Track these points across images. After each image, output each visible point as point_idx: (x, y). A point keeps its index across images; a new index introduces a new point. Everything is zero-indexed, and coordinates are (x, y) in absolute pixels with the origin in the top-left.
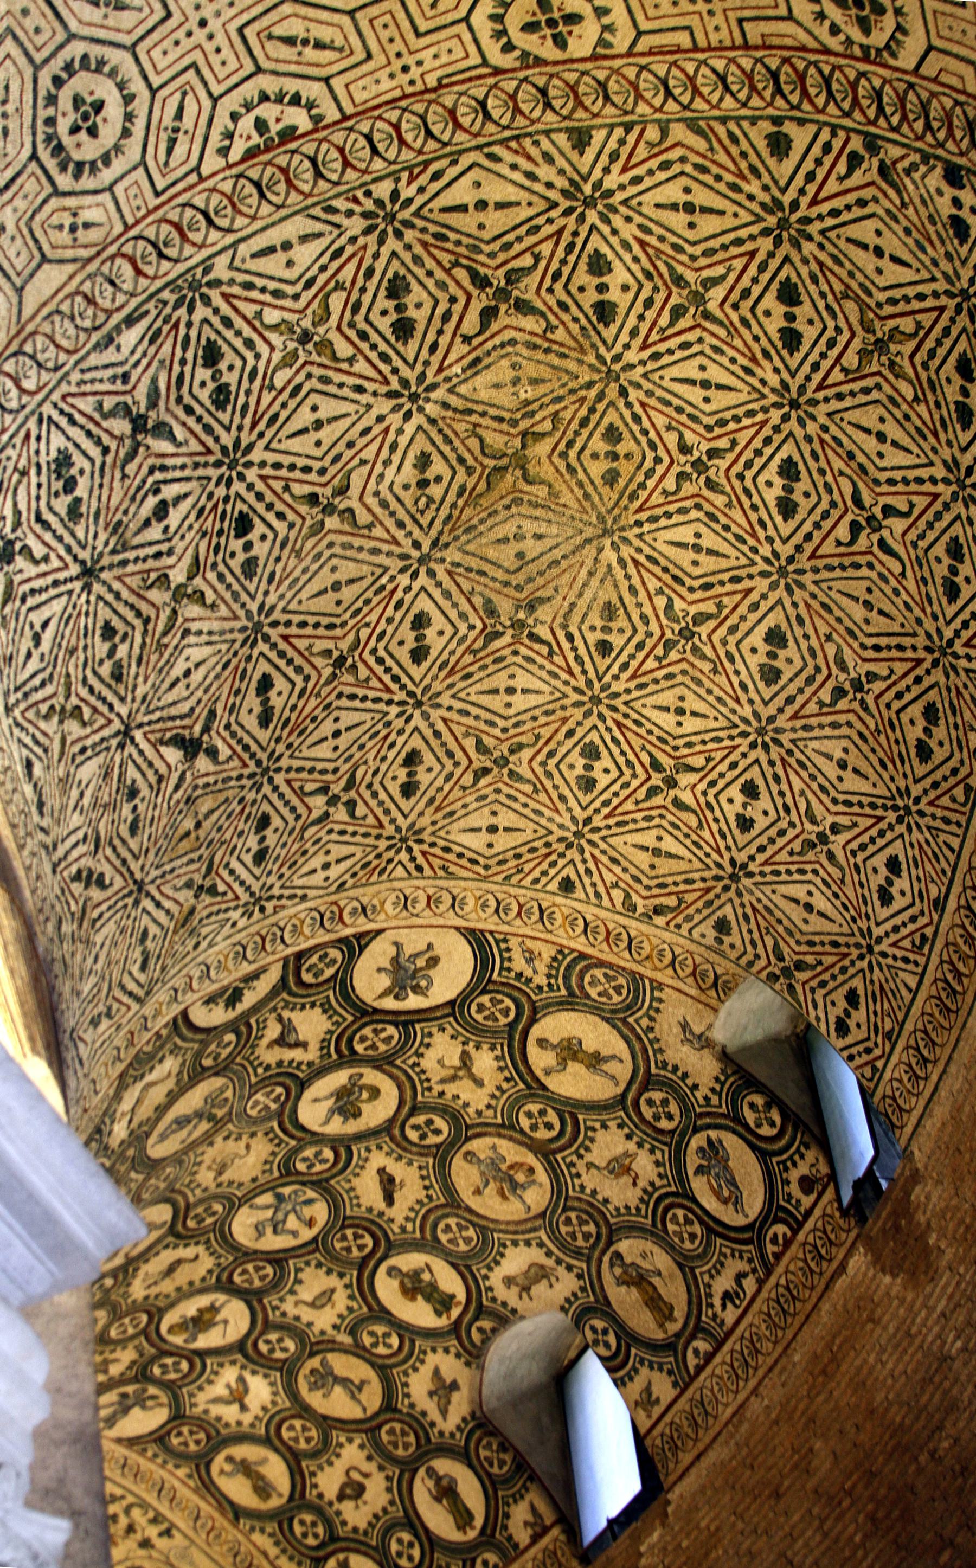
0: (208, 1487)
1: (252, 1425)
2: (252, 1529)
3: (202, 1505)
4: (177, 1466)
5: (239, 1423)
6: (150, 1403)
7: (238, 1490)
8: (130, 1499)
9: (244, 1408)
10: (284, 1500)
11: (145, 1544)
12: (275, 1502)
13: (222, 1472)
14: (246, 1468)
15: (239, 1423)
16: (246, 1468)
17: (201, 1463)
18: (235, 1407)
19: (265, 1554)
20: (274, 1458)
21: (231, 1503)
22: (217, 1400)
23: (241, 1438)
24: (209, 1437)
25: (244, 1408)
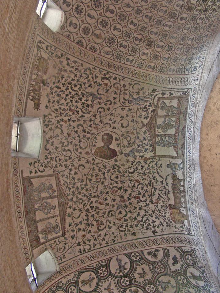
0: (88, 269)
1: (100, 289)
2: (75, 275)
3: (85, 265)
4: (97, 265)
5: (102, 286)
6: (118, 271)
7: (85, 276)
8: (92, 248)
9: (105, 289)
10: (80, 287)
11: (79, 244)
12: (80, 284)
13: (91, 275)
14: (90, 281)
15: (102, 286)
16: (90, 281)
17: (95, 271)
18: (106, 288)
19: (68, 275)
20: (91, 290)
21: (83, 272)
22: (110, 284)
23: (98, 284)
24: (101, 277)
25: (105, 289)
